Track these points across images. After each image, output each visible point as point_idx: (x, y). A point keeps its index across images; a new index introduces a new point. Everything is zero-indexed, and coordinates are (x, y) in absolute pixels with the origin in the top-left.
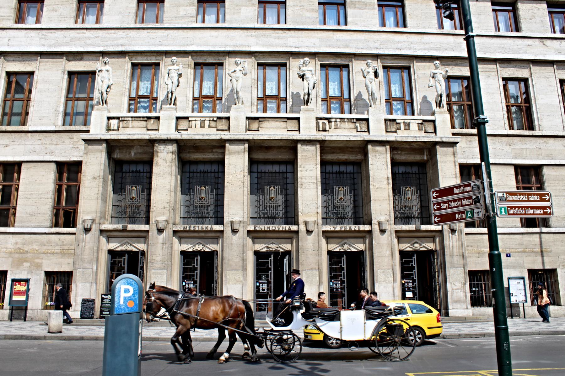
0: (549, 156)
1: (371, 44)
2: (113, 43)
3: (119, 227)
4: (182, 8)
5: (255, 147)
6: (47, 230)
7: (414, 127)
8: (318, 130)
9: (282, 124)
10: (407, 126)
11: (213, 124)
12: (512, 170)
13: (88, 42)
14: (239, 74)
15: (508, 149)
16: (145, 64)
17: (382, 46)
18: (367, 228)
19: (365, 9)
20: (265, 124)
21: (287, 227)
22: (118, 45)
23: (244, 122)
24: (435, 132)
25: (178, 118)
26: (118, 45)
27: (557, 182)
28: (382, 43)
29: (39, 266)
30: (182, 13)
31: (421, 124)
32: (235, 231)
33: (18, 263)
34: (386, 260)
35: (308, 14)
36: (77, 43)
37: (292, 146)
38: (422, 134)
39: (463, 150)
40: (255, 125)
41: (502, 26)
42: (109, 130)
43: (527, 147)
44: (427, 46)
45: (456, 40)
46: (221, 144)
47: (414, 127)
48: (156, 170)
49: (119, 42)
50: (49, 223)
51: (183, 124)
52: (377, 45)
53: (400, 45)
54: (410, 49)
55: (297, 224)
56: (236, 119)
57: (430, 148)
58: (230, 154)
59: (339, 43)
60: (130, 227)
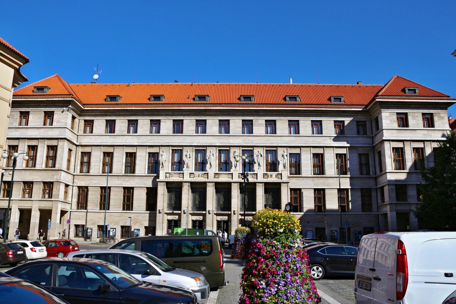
0: (328, 185)
2: (165, 141)
3: (171, 212)
4: (190, 127)
5: (217, 184)
7: (274, 176)
8: (239, 177)
9: (227, 176)
10: (271, 176)
11: (202, 176)
12: (313, 191)
13: (155, 141)
14: (212, 156)
15: (312, 182)
16: (178, 151)
17: (266, 142)
18: (254, 213)
20: (221, 176)
21: (227, 212)
22: (167, 143)
23: (213, 175)
24: (281, 178)
25: (190, 173)
26: (167, 143)
29: (142, 224)
30: (190, 129)
32: (209, 213)
33: (136, 223)
35: (238, 129)
36: (151, 141)
37: (229, 184)
38: (277, 179)
40: (217, 176)
41: (315, 133)
42: (166, 177)
44: (283, 142)
46: (205, 183)
47: (274, 176)
48: (183, 192)
49: (167, 141)
50: (145, 209)
51: (192, 176)
52: (264, 142)
53: (273, 142)
54: (276, 143)
55: (231, 211)
56: (210, 173)
57: (279, 184)
58: (209, 187)
59: (249, 142)
60: (175, 212)
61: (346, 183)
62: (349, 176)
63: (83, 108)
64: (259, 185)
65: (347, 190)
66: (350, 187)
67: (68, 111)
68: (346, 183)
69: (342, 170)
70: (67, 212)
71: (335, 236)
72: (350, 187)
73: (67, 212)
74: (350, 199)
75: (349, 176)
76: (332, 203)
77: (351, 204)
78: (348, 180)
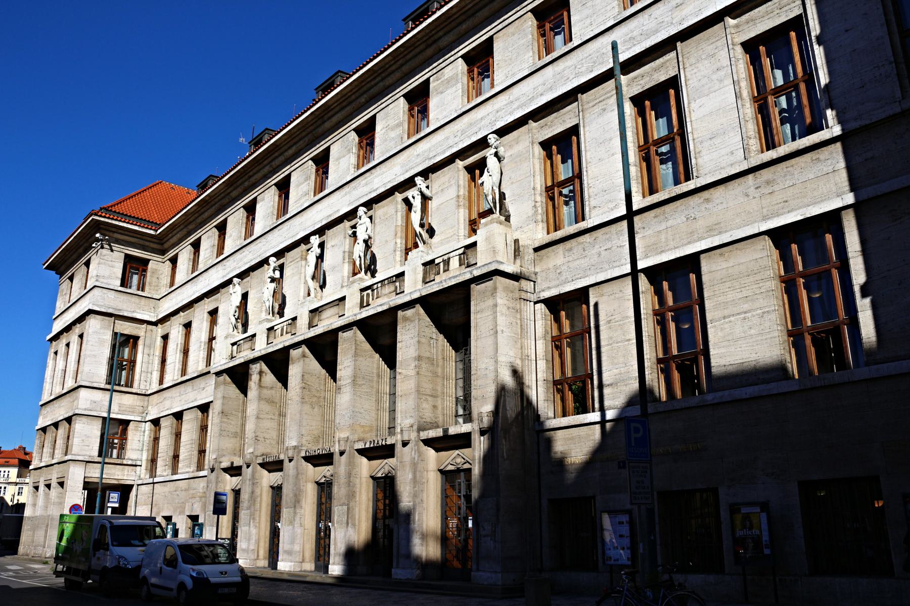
1: (451, 142)
6: (191, 475)
19: (447, 88)
27: (728, 284)
28: (463, 132)
31: (464, 253)
34: (408, 488)
39: (558, 271)
43: (670, 223)
45: (556, 69)
61: (821, 185)
62: (837, 130)
63: (152, 232)
64: (406, 319)
65: (832, 220)
66: (850, 199)
67: (102, 247)
68: (821, 185)
69: (784, 112)
70: (133, 486)
71: (757, 541)
72: (850, 199)
73: (133, 486)
74: (859, 276)
75: (837, 130)
76: (747, 329)
77: (875, 308)
78: (834, 161)
